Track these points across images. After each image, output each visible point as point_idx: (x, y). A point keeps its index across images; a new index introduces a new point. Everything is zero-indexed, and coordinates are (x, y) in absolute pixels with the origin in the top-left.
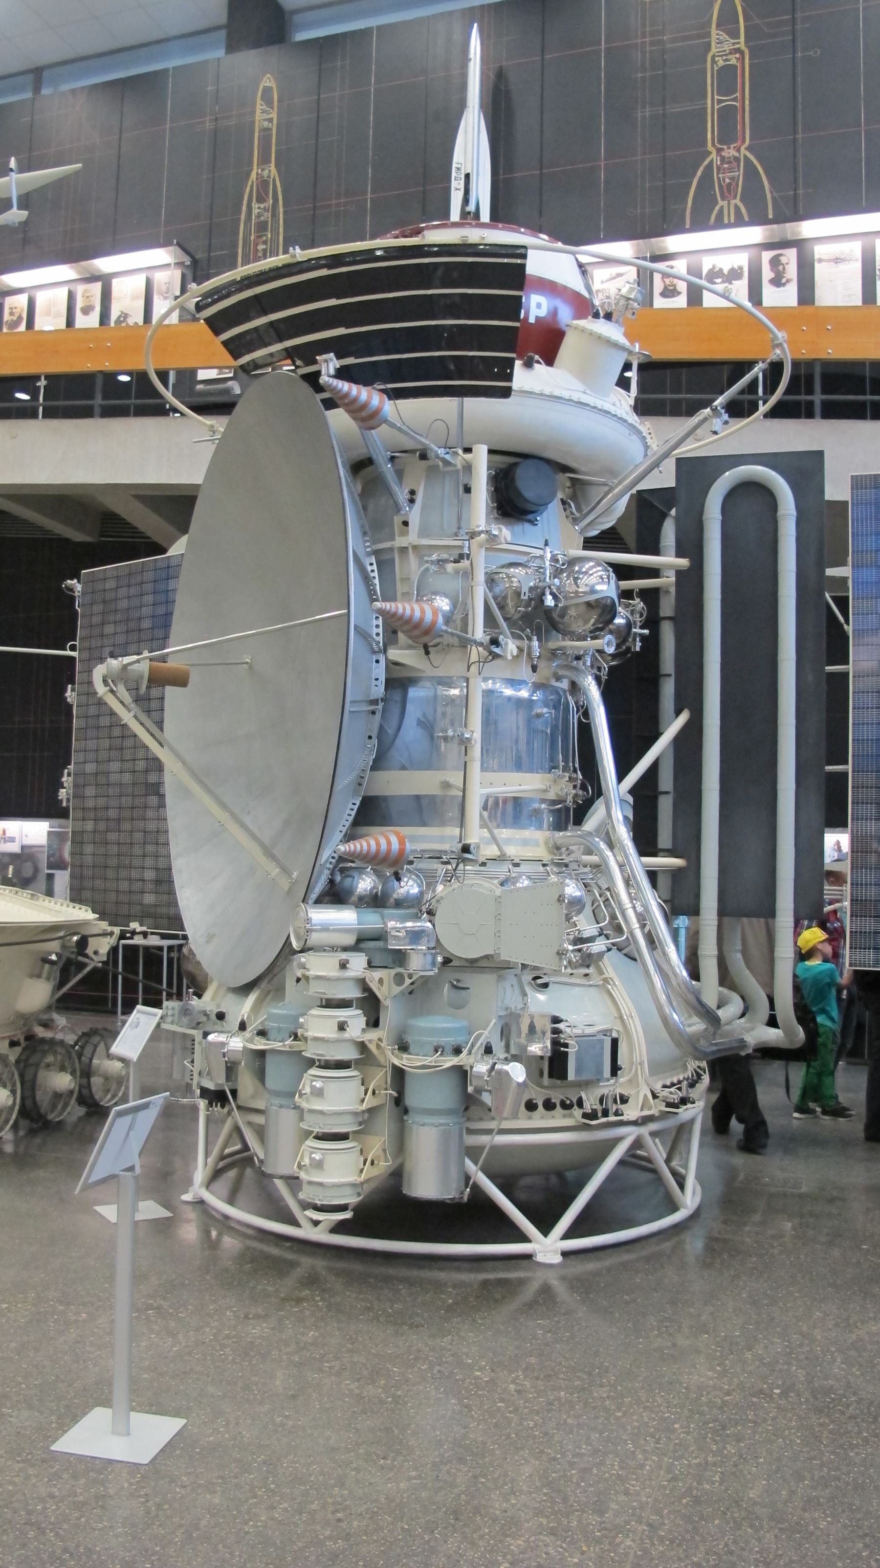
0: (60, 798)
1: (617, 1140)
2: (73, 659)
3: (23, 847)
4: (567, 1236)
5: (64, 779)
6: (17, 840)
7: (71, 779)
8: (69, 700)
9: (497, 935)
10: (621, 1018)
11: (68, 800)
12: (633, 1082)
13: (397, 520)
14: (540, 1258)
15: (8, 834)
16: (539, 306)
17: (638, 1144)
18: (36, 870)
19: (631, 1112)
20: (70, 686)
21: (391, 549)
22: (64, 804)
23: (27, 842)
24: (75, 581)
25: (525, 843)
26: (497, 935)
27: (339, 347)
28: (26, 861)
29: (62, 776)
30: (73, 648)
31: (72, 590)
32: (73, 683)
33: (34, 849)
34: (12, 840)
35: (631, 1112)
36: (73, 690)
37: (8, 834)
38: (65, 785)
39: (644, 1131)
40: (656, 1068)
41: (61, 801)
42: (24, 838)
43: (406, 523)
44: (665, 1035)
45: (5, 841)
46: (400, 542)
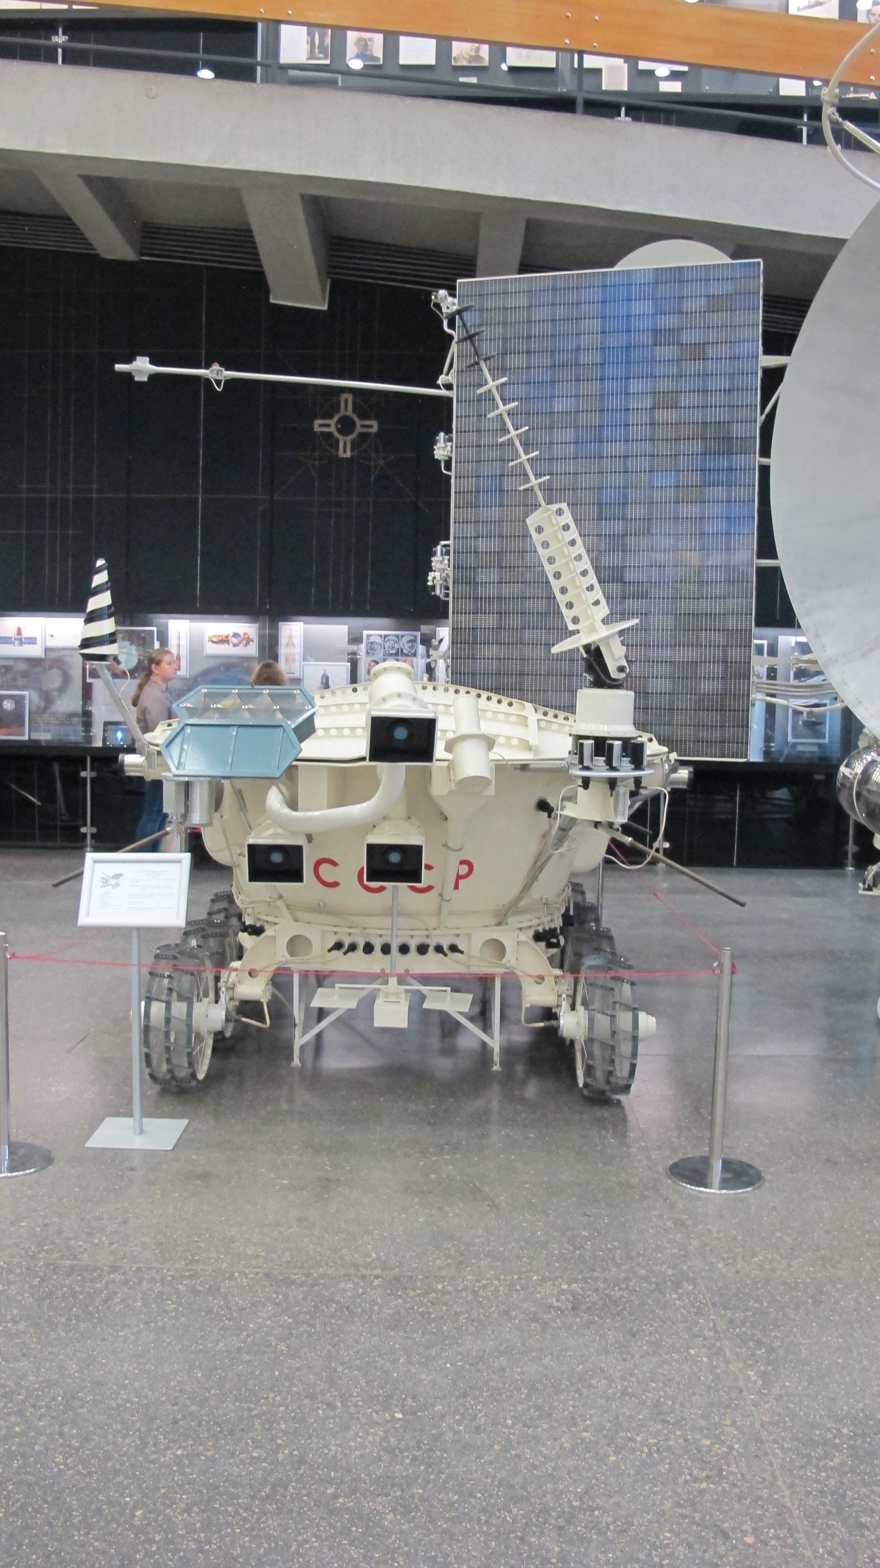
0: (430, 583)
2: (450, 400)
3: (47, 650)
6: (39, 641)
15: (25, 634)
18: (67, 679)
23: (51, 643)
28: (51, 667)
31: (438, 306)
32: (449, 431)
33: (63, 653)
34: (32, 641)
37: (25, 634)
41: (433, 588)
42: (48, 638)
45: (21, 643)
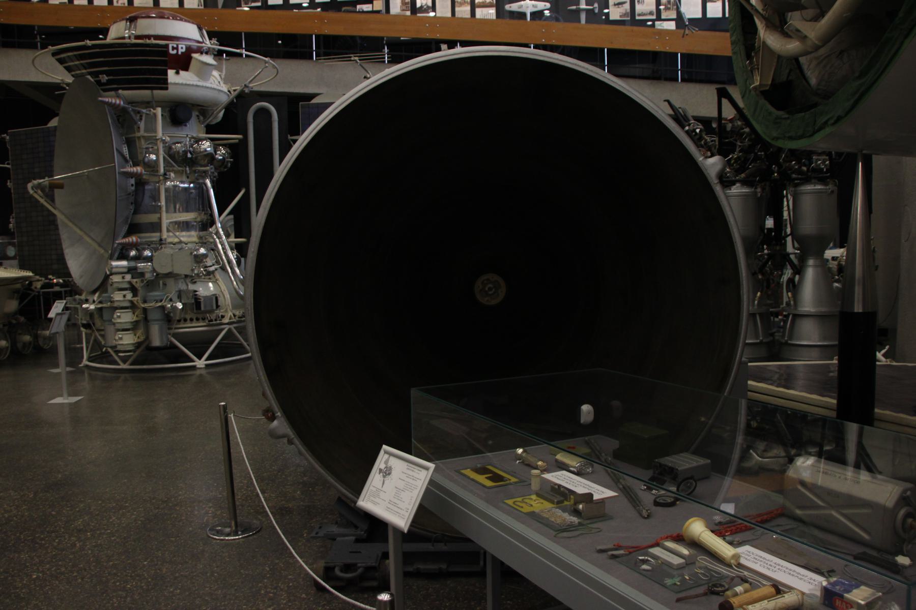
1: (223, 329)
2: (8, 169)
4: (207, 360)
5: (11, 220)
7: (14, 220)
8: (9, 186)
9: (172, 266)
10: (222, 291)
11: (14, 229)
12: (226, 311)
13: (136, 127)
14: (198, 366)
16: (182, 48)
17: (230, 330)
19: (226, 320)
20: (9, 181)
21: (135, 137)
22: (12, 230)
24: (5, 135)
25: (189, 236)
26: (172, 266)
27: (108, 73)
29: (10, 219)
30: (8, 164)
35: (226, 320)
36: (10, 182)
38: (12, 222)
39: (232, 327)
40: (235, 307)
41: (11, 229)
43: (139, 128)
44: (238, 298)
46: (138, 134)
